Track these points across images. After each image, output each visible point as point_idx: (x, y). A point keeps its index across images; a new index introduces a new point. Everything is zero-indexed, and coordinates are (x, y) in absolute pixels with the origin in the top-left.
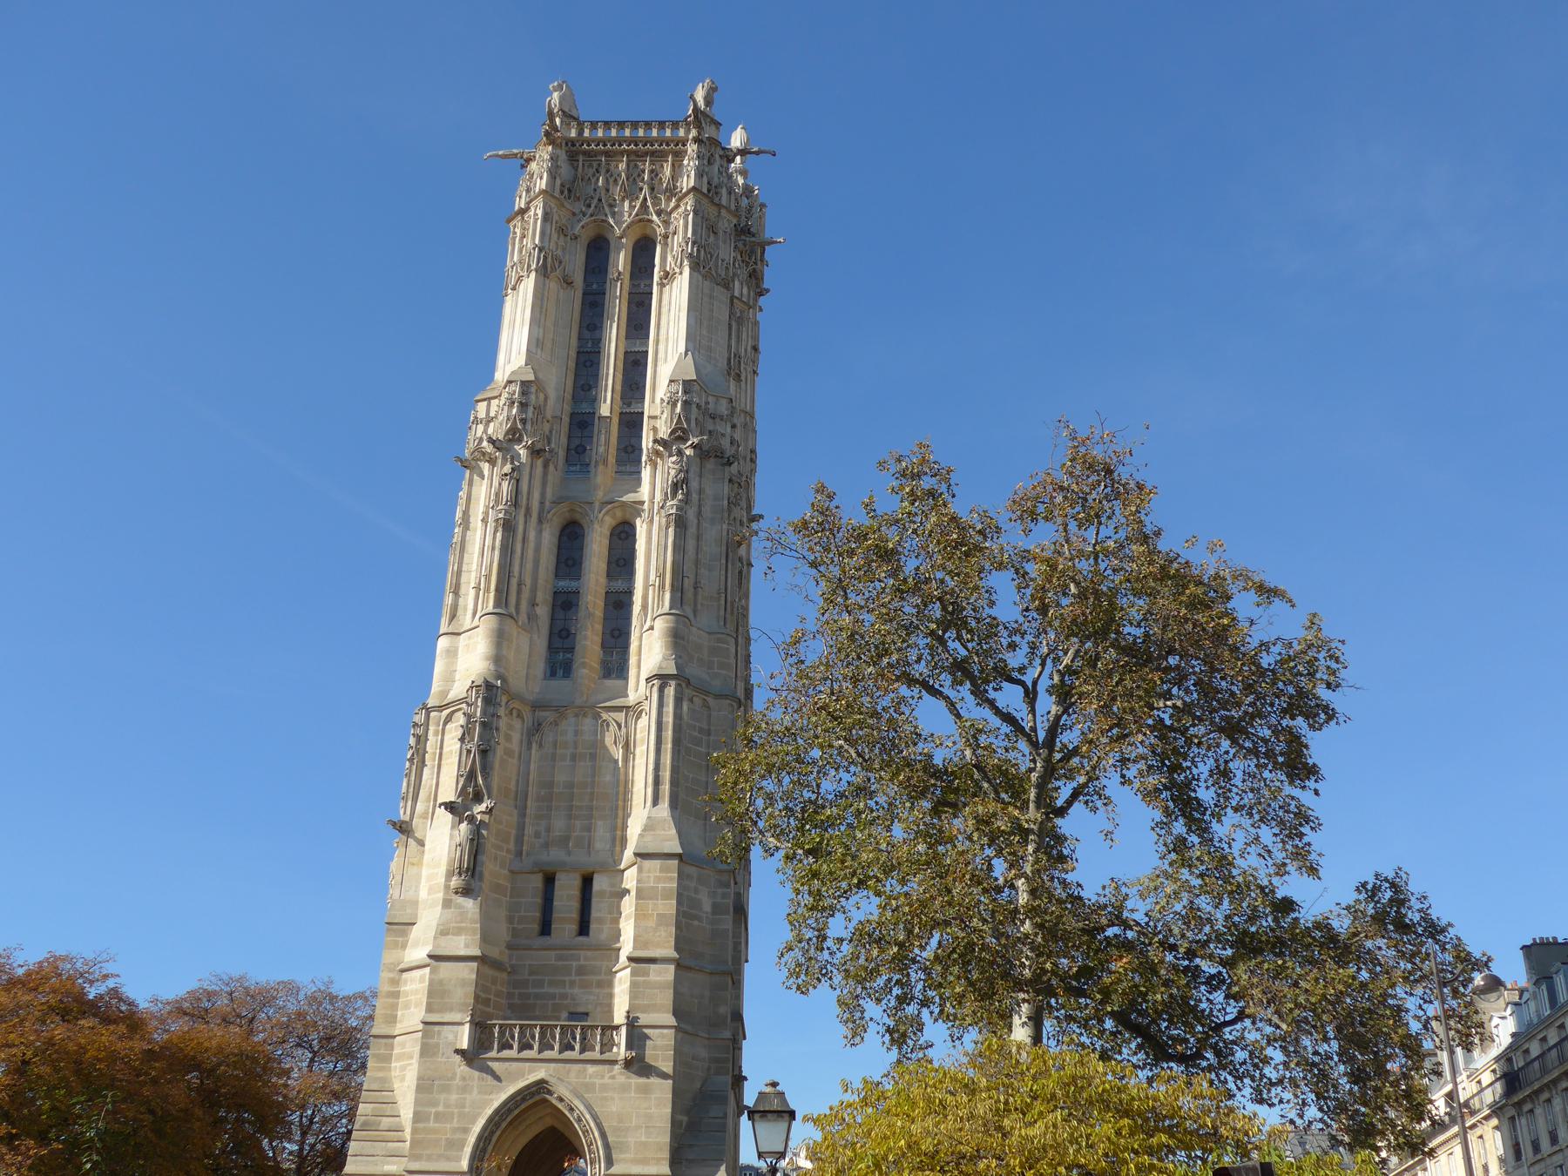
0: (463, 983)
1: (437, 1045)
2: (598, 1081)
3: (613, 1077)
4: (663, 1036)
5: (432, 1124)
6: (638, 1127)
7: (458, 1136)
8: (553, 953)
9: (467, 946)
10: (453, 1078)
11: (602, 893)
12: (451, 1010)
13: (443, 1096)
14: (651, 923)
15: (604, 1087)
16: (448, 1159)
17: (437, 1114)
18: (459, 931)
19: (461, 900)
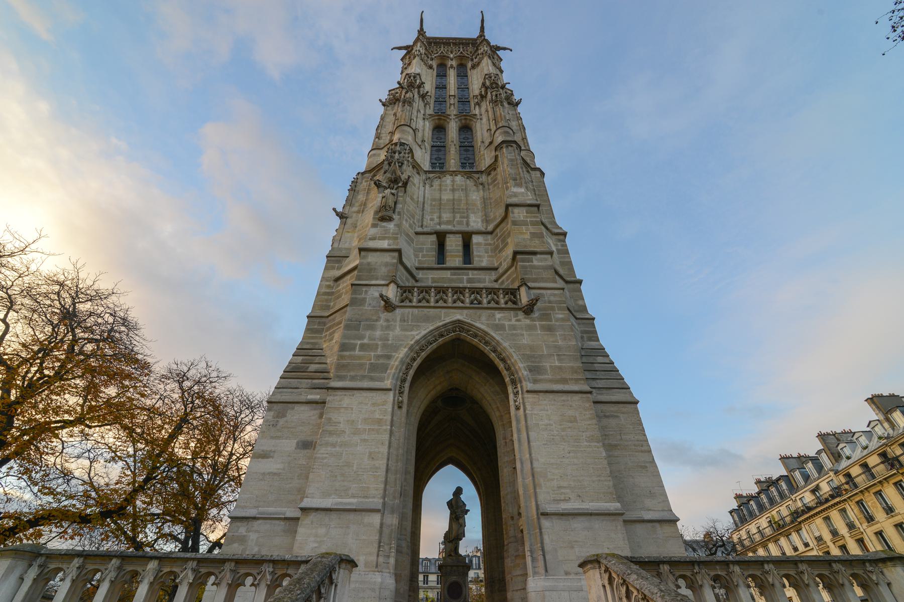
0: (387, 264)
1: (364, 300)
2: (507, 323)
3: (518, 320)
4: (555, 295)
5: (357, 352)
6: (551, 355)
7: (381, 361)
8: (449, 272)
9: (389, 245)
10: (377, 320)
11: (479, 244)
12: (377, 279)
13: (368, 333)
14: (527, 236)
15: (513, 327)
16: (372, 379)
17: (363, 347)
18: (383, 238)
19: (384, 224)
